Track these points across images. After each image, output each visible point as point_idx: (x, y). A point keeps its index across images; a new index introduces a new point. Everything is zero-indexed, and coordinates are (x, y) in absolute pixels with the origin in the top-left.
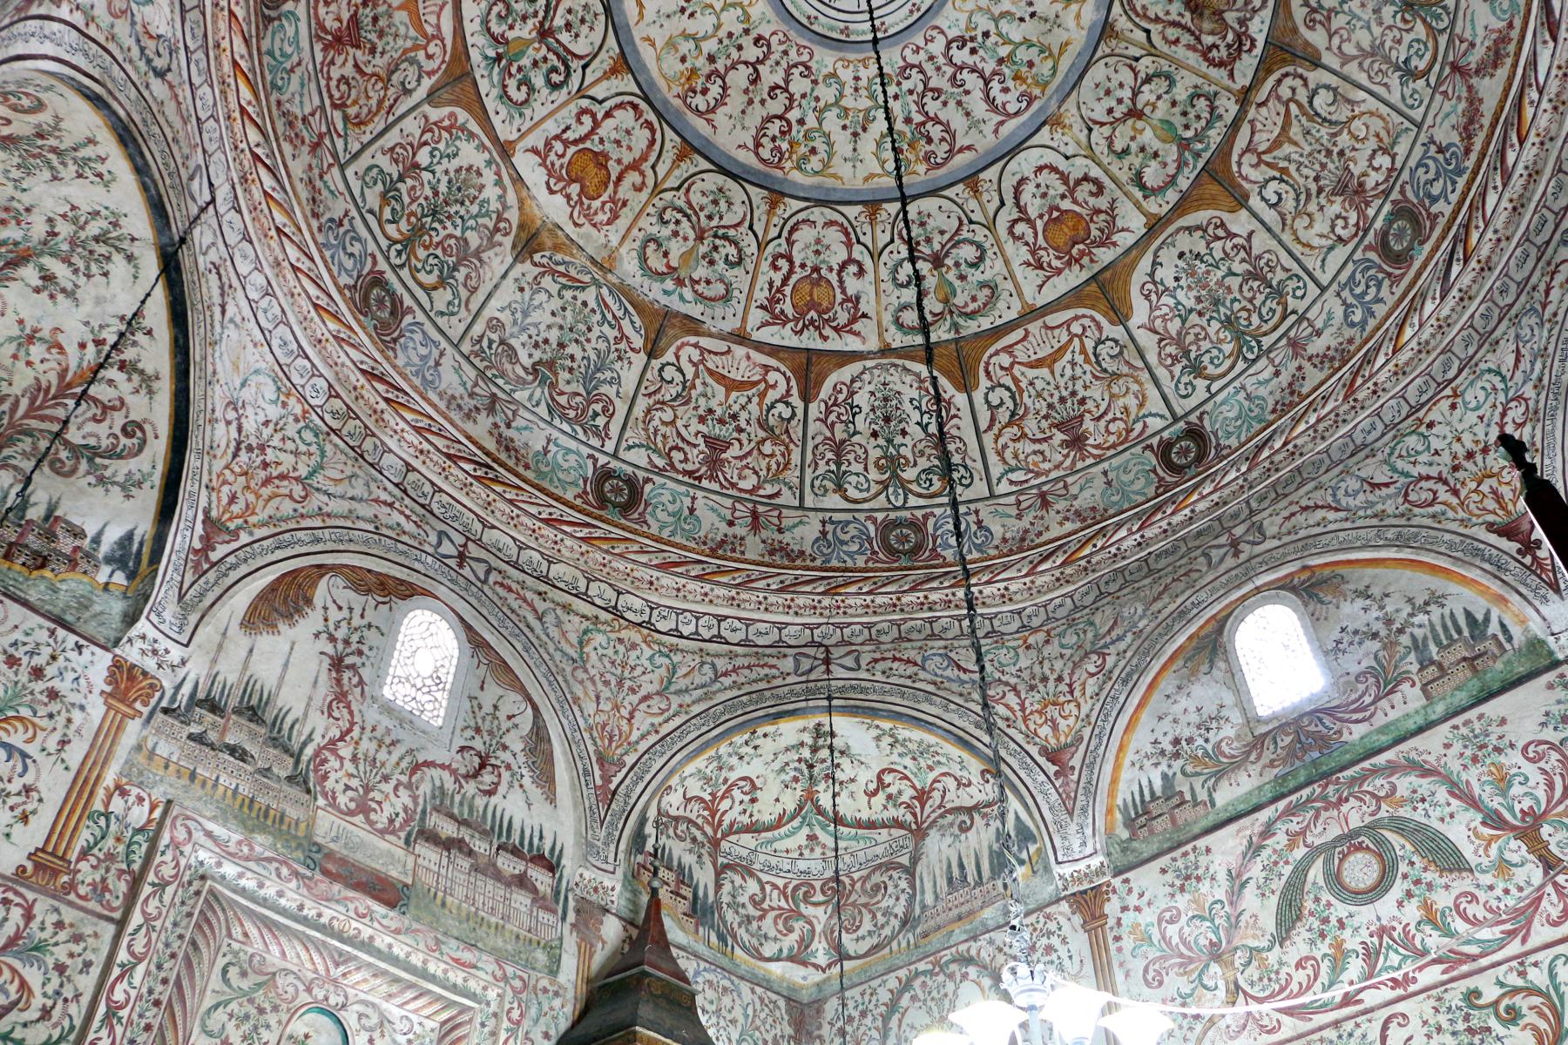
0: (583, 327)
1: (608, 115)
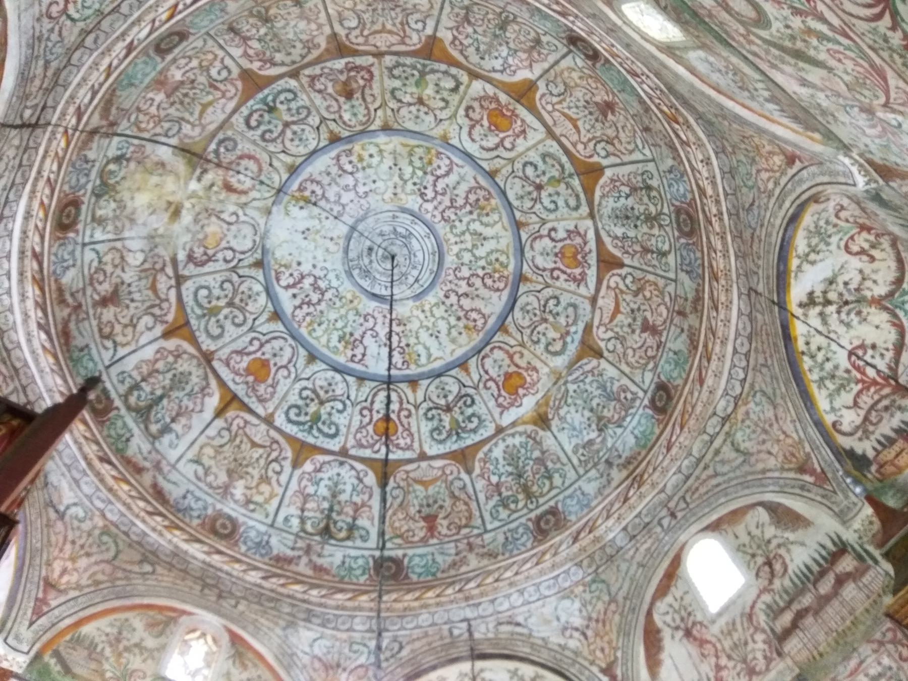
0: (585, 395)
1: (487, 372)
